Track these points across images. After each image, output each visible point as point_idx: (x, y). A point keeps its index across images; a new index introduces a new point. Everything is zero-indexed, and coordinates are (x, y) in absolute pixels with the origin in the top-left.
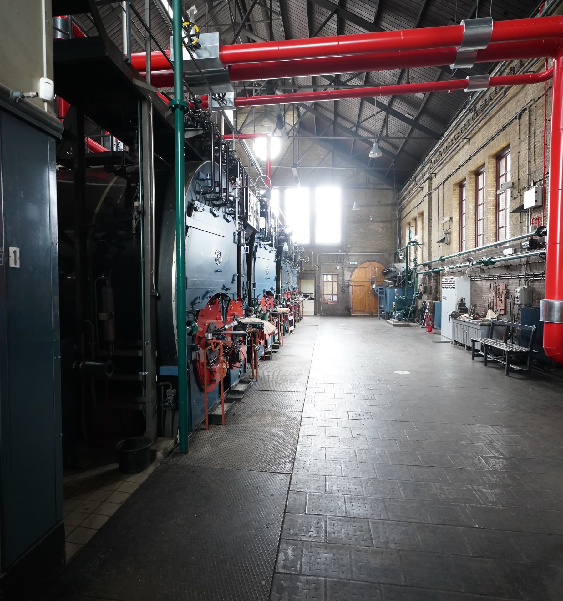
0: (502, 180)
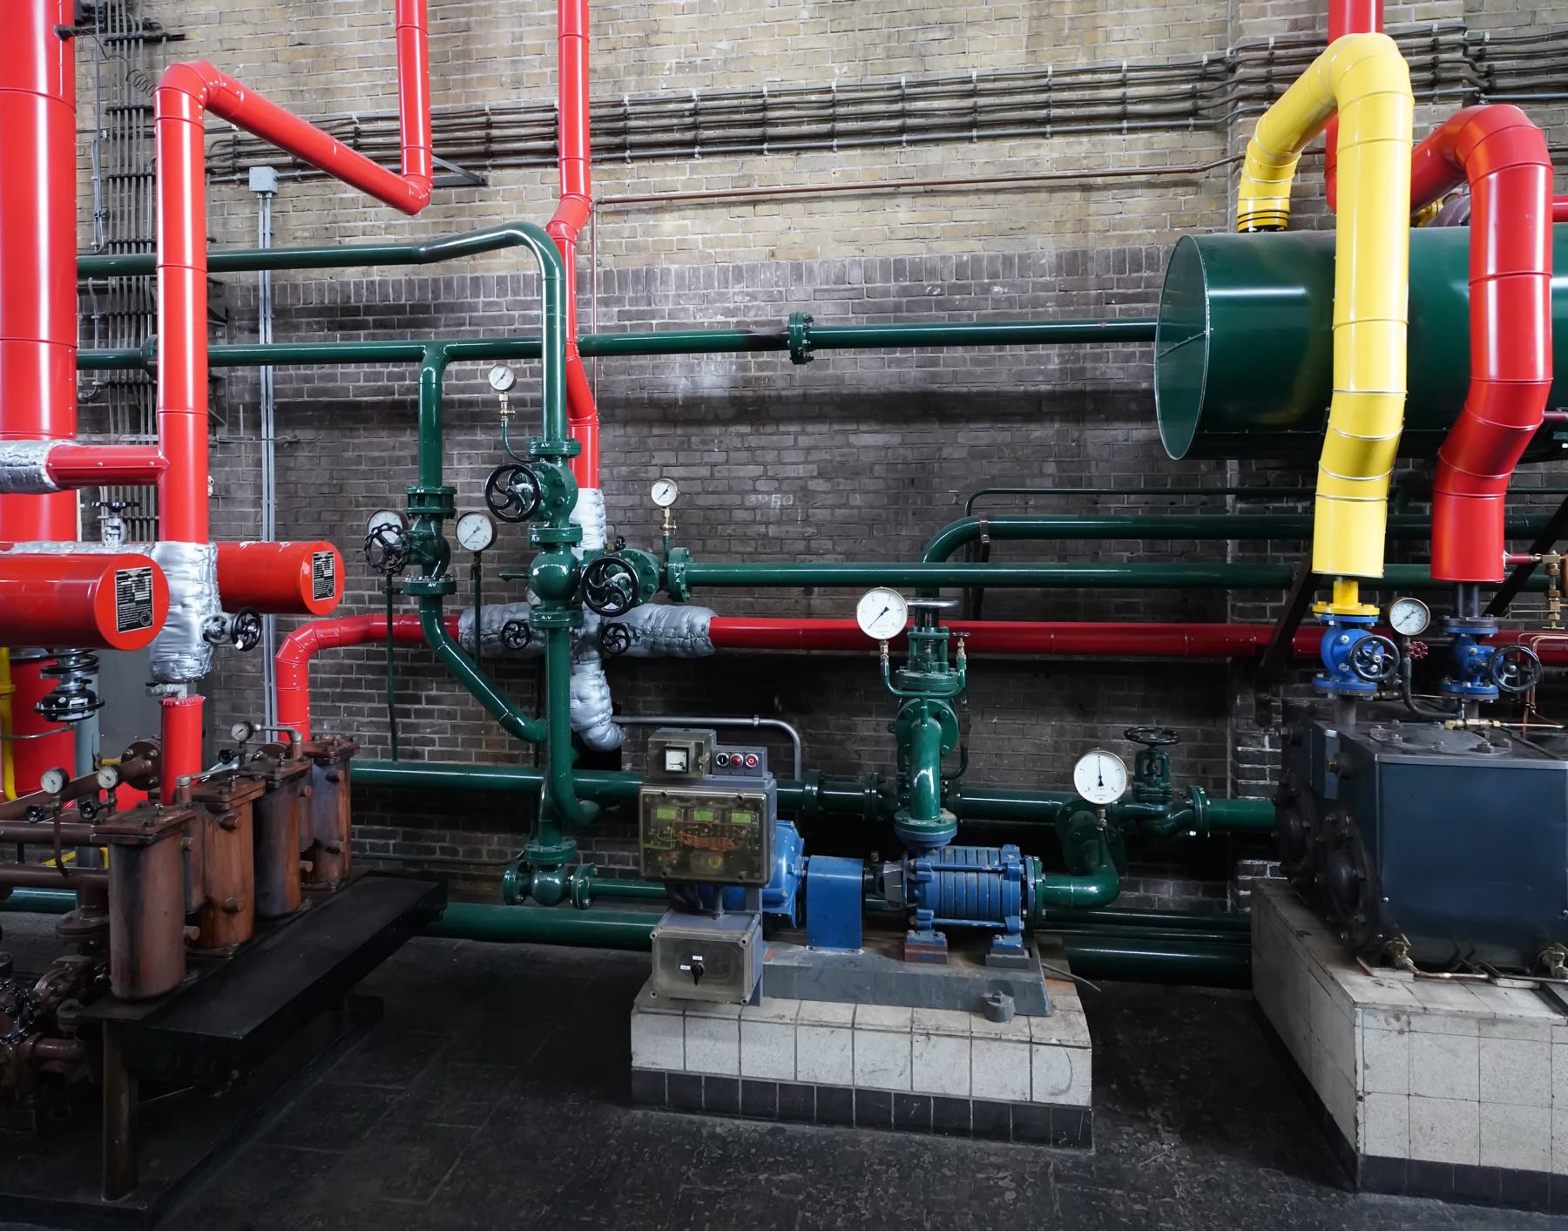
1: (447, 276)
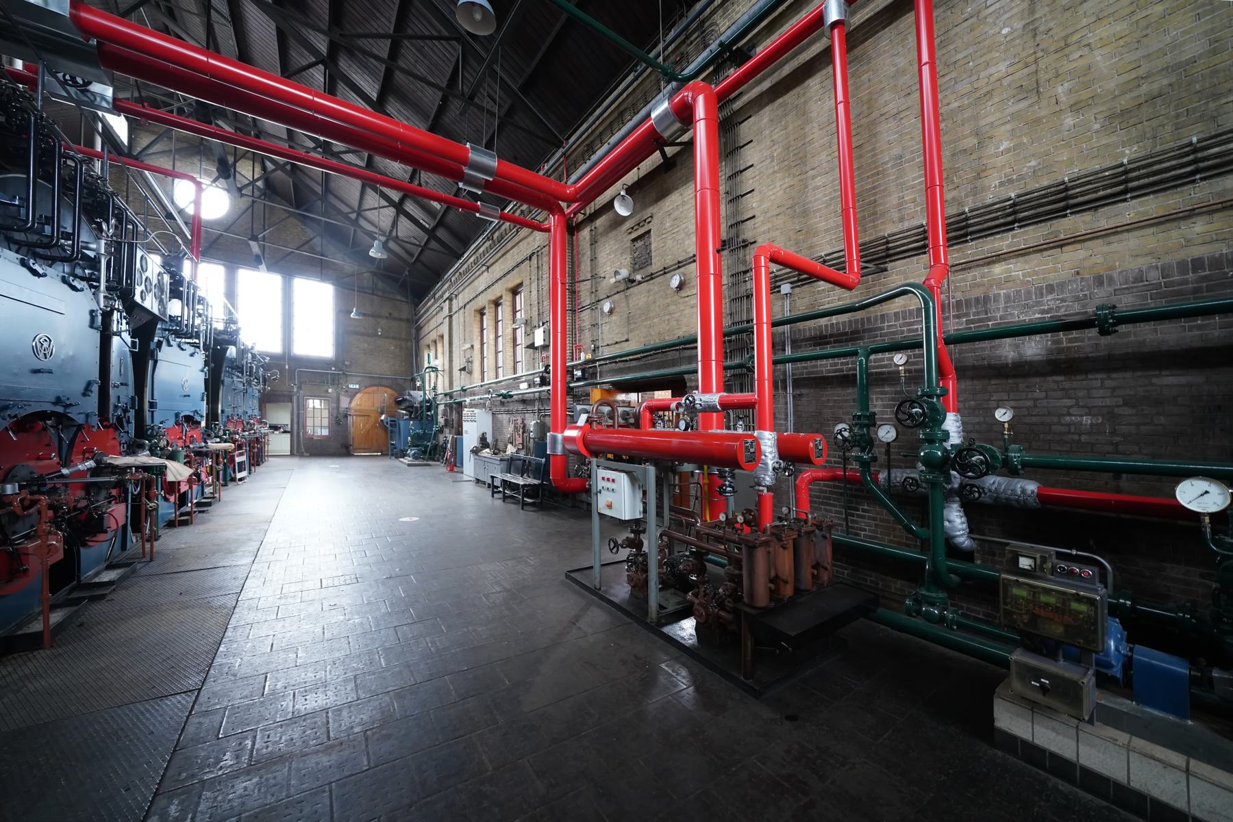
0: (518, 315)
1: (868, 316)
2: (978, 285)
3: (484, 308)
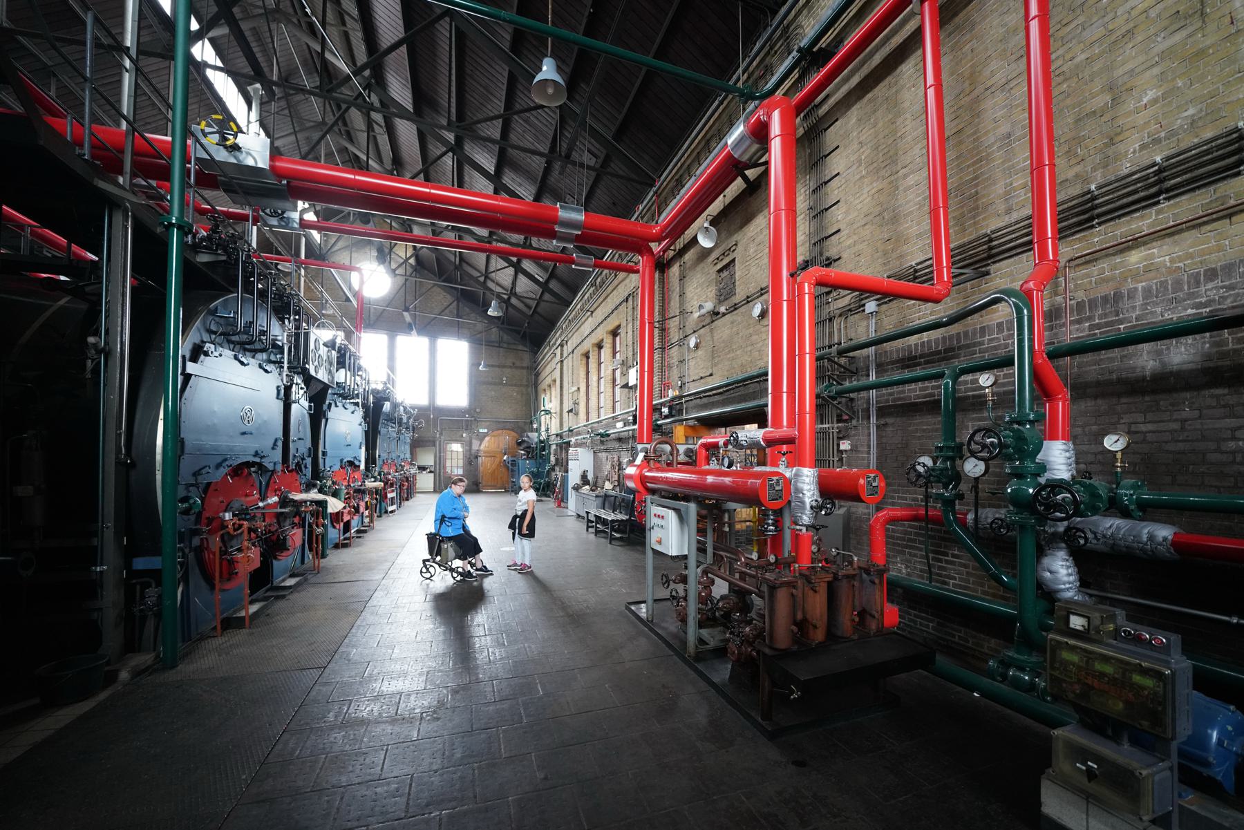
2: (1106, 280)
3: (589, 352)
